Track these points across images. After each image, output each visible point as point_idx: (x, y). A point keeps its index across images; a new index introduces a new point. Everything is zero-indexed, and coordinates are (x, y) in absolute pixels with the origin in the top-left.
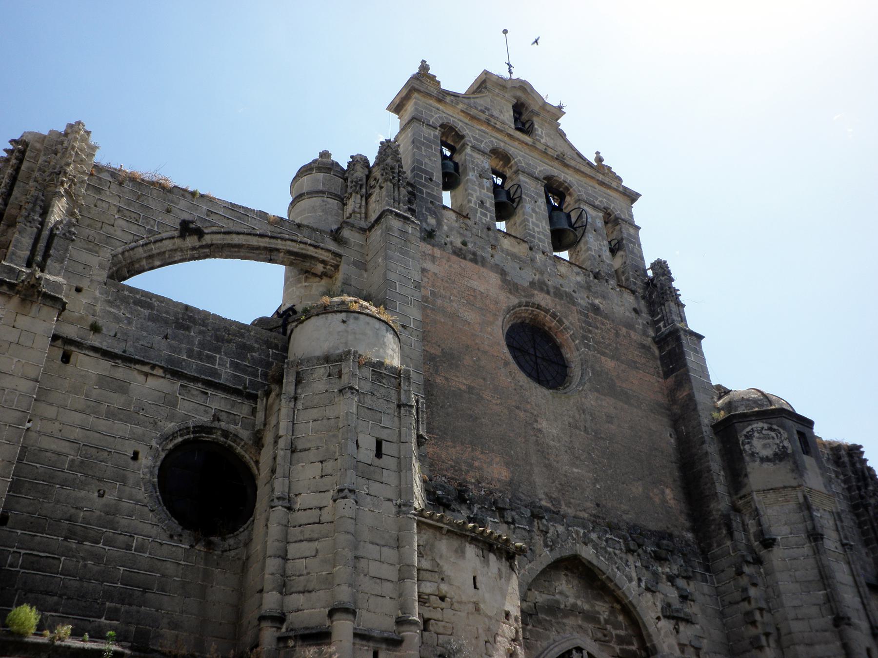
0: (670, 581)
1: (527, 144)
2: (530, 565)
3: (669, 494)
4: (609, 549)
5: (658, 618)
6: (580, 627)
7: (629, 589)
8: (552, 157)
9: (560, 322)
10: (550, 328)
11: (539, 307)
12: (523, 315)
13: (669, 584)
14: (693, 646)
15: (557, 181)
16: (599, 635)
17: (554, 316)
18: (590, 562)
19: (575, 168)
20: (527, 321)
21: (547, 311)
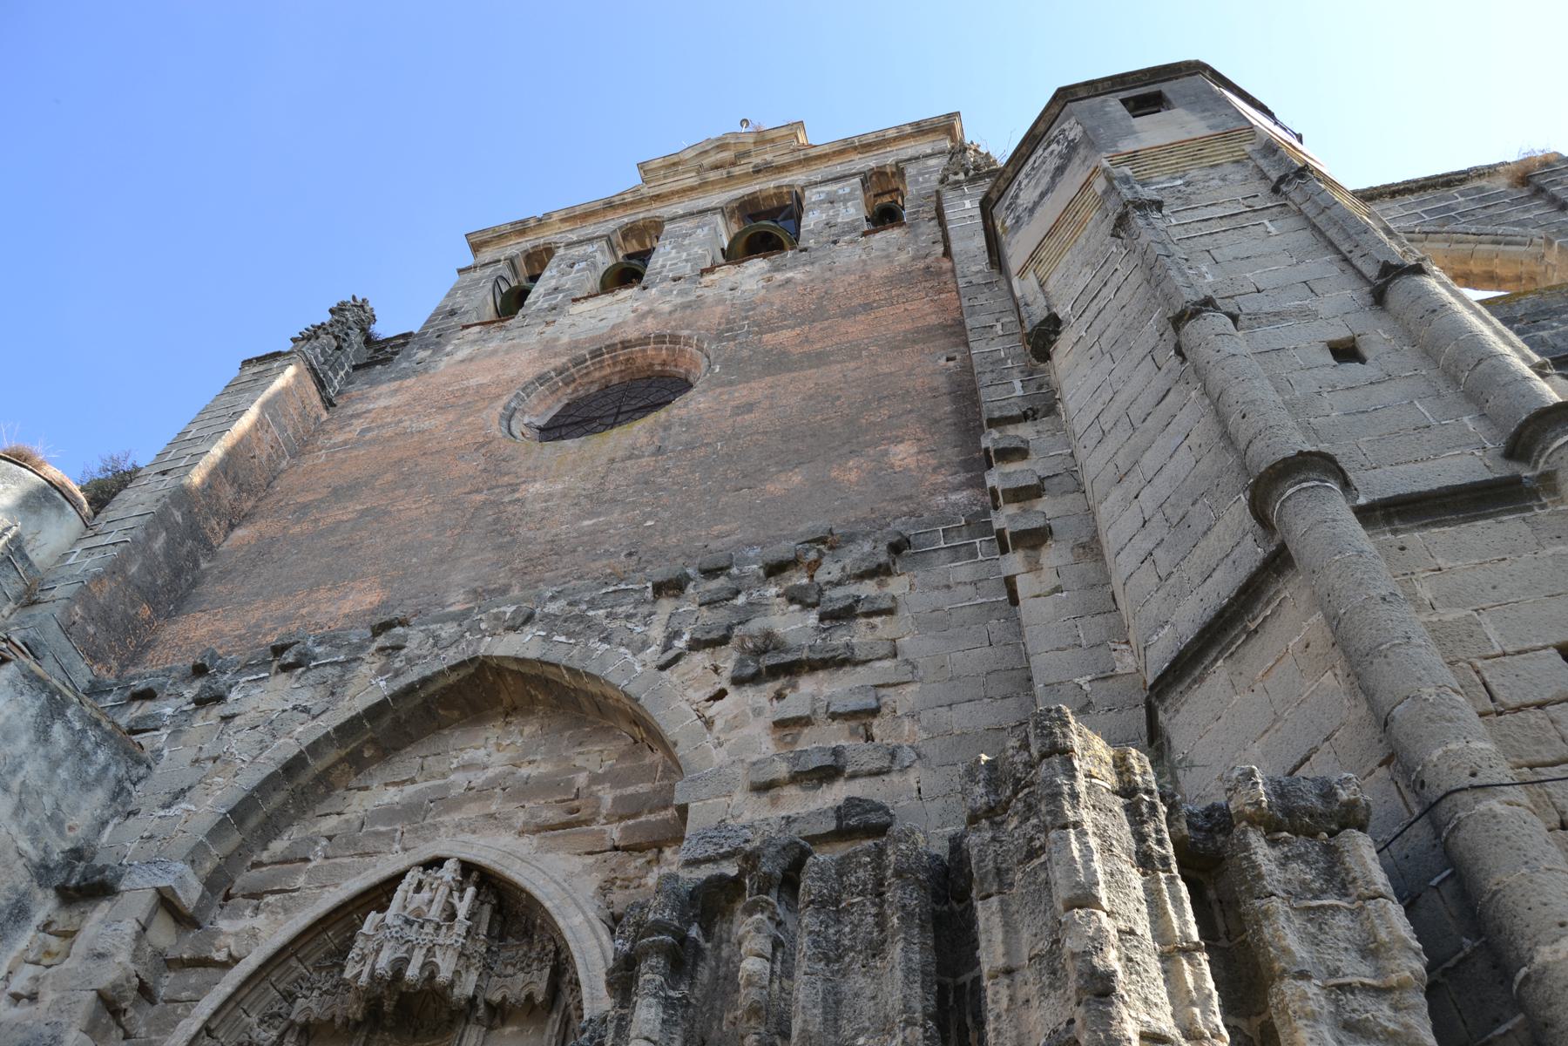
0: (792, 600)
1: (692, 189)
2: (314, 723)
3: (903, 454)
4: (591, 613)
5: (721, 694)
6: (492, 816)
7: (627, 669)
8: (747, 174)
9: (675, 339)
10: (664, 364)
11: (625, 344)
12: (597, 374)
13: (797, 607)
14: (834, 716)
15: (769, 197)
16: (552, 815)
17: (660, 339)
18: (517, 660)
19: (799, 162)
20: (616, 380)
21: (644, 341)
